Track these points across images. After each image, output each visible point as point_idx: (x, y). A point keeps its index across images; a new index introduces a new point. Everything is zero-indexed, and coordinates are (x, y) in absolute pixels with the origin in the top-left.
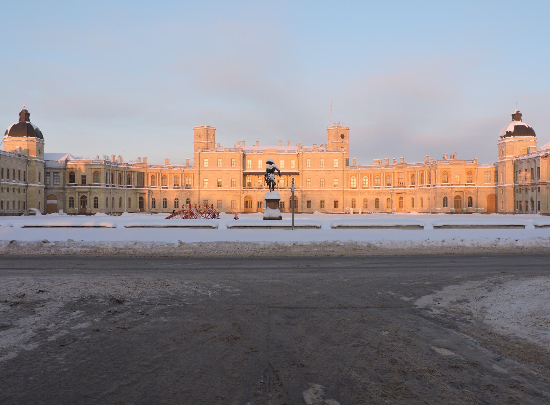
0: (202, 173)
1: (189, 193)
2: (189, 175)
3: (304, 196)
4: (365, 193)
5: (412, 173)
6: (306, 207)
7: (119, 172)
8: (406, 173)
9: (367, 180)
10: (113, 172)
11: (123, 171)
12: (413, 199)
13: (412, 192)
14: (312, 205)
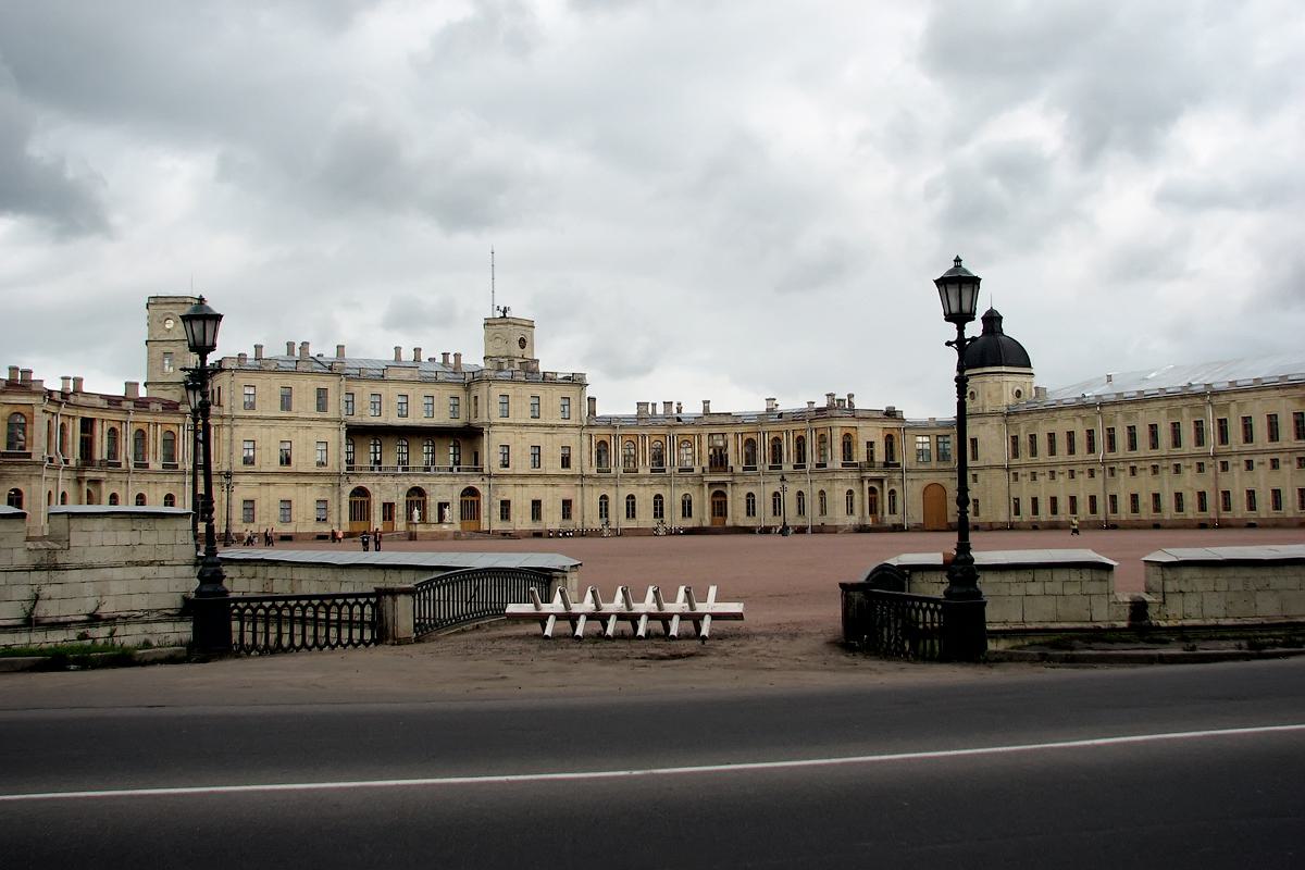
5: (749, 436)
8: (731, 437)
11: (53, 414)
14: (513, 511)
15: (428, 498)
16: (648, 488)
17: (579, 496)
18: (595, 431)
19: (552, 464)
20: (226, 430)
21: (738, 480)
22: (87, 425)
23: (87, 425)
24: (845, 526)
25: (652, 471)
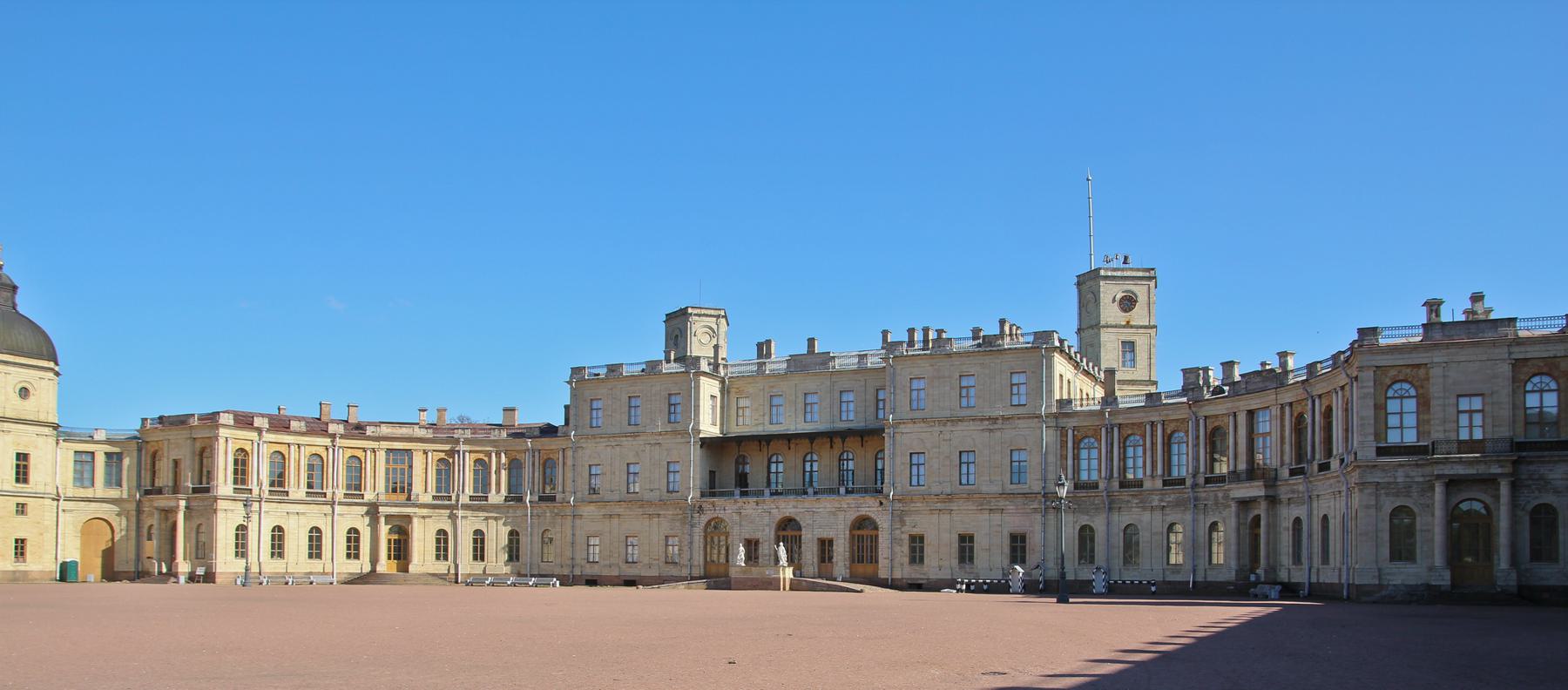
0: (584, 445)
1: (548, 514)
2: (551, 456)
3: (899, 518)
4: (1128, 501)
6: (906, 560)
7: (314, 450)
9: (1140, 451)
10: (283, 449)
12: (1298, 521)
13: (1298, 492)
15: (803, 532)
16: (1158, 516)
17: (1038, 528)
18: (1072, 423)
19: (990, 480)
20: (569, 453)
21: (1283, 492)
22: (400, 458)
23: (400, 458)
24: (1381, 586)
25: (1165, 483)
